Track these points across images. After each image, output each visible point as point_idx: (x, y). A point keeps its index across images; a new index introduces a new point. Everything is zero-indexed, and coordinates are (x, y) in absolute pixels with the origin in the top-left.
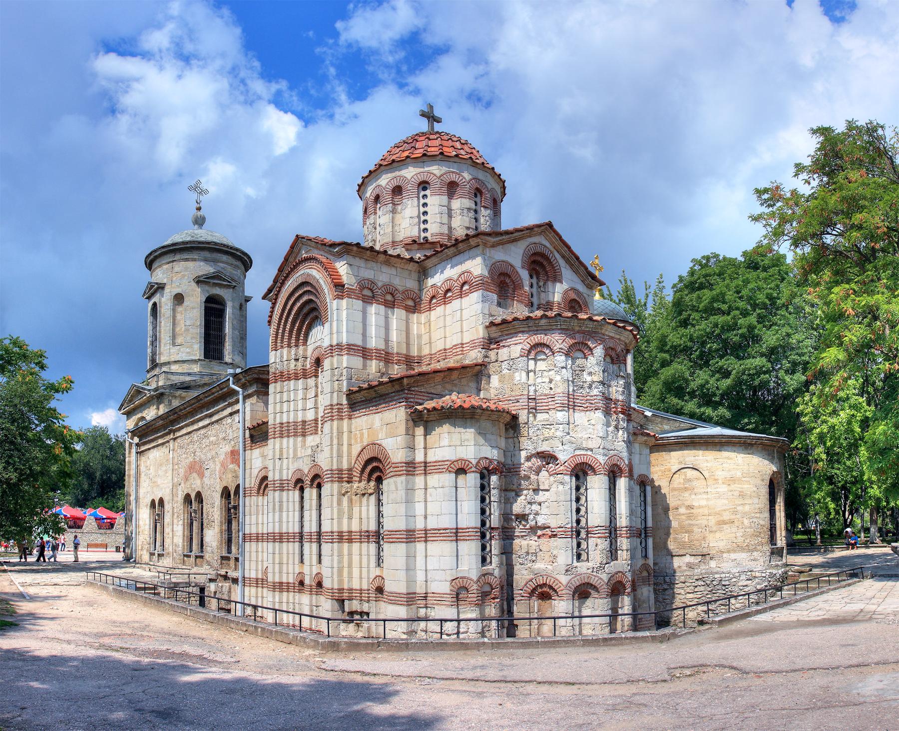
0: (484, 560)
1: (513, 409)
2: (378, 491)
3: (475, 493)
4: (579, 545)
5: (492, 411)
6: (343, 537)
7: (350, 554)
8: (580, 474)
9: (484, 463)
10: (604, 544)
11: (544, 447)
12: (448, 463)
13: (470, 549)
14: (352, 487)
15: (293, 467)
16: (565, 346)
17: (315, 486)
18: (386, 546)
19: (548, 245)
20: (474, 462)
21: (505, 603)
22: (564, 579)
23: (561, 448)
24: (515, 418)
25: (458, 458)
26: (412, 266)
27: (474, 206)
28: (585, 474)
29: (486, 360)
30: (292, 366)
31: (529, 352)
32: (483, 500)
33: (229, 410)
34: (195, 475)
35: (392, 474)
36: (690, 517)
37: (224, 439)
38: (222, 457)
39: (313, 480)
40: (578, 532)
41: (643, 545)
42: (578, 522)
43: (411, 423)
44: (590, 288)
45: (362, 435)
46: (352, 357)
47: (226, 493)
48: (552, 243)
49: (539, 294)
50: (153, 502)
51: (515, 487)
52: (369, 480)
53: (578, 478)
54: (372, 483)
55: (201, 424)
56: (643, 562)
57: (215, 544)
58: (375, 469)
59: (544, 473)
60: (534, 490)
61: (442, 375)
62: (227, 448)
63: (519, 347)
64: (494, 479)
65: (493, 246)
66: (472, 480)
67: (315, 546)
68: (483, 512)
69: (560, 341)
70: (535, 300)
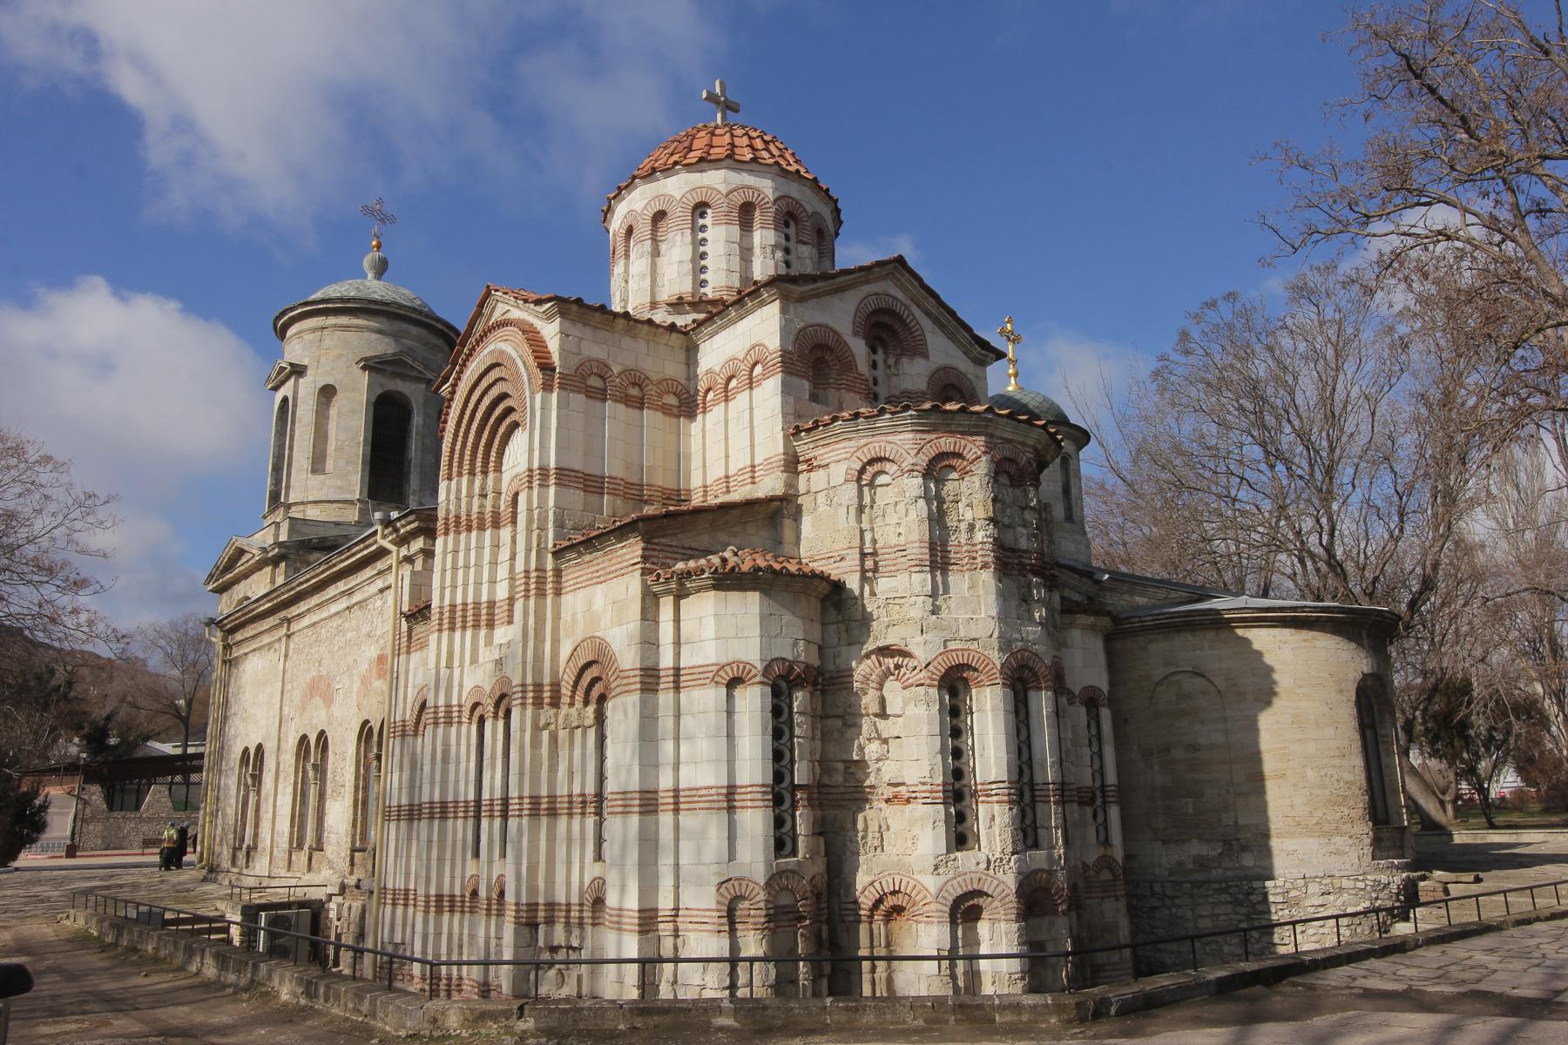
1: (834, 571)
2: (600, 719)
5: (792, 575)
9: (777, 669)
12: (715, 668)
13: (755, 822)
14: (556, 715)
16: (923, 461)
17: (501, 714)
20: (759, 666)
21: (825, 928)
23: (919, 639)
25: (730, 660)
30: (475, 508)
31: (862, 471)
32: (777, 734)
33: (380, 584)
34: (318, 700)
35: (618, 690)
37: (369, 635)
38: (364, 667)
39: (497, 705)
40: (957, 792)
44: (982, 363)
46: (564, 490)
47: (365, 732)
49: (888, 377)
51: (840, 712)
53: (954, 693)
54: (591, 709)
55: (334, 608)
59: (891, 686)
60: (876, 715)
61: (709, 516)
62: (371, 652)
63: (843, 467)
64: (799, 699)
68: (777, 756)
69: (913, 452)
70: (882, 391)
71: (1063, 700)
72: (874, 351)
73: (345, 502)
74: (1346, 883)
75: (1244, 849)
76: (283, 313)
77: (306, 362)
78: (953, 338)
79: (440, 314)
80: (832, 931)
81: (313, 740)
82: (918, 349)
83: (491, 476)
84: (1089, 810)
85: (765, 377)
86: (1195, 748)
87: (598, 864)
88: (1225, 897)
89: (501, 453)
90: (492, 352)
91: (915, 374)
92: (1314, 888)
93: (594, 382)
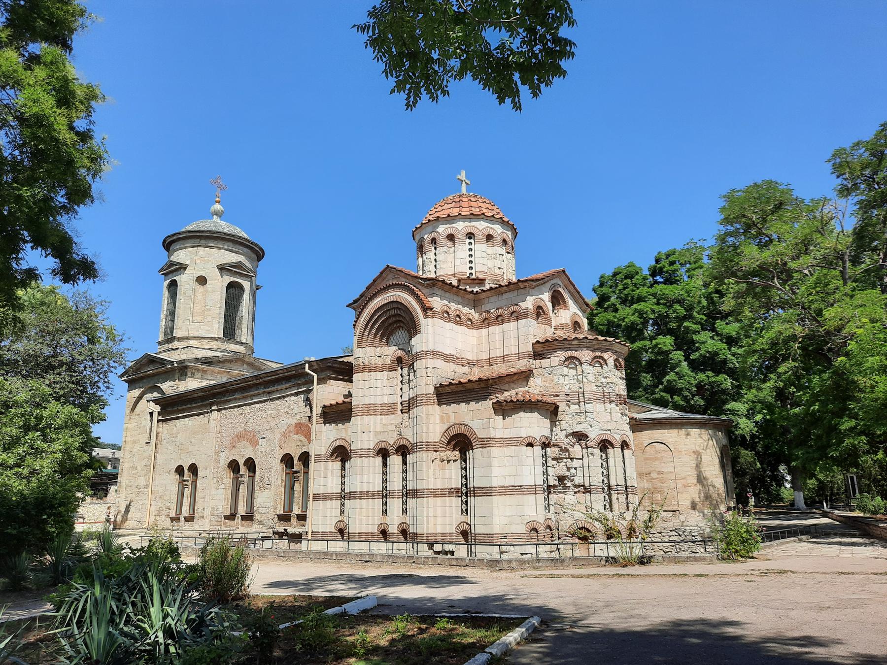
3: (540, 460)
6: (436, 493)
7: (435, 507)
11: (578, 428)
15: (380, 438)
18: (471, 500)
23: (590, 429)
24: (557, 407)
29: (533, 366)
36: (660, 480)
38: (284, 428)
45: (448, 417)
50: (180, 470)
57: (270, 505)
58: (461, 443)
66: (538, 449)
73: (211, 338)
76: (173, 235)
77: (188, 263)
78: (576, 302)
81: (241, 462)
82: (566, 307)
88: (674, 533)
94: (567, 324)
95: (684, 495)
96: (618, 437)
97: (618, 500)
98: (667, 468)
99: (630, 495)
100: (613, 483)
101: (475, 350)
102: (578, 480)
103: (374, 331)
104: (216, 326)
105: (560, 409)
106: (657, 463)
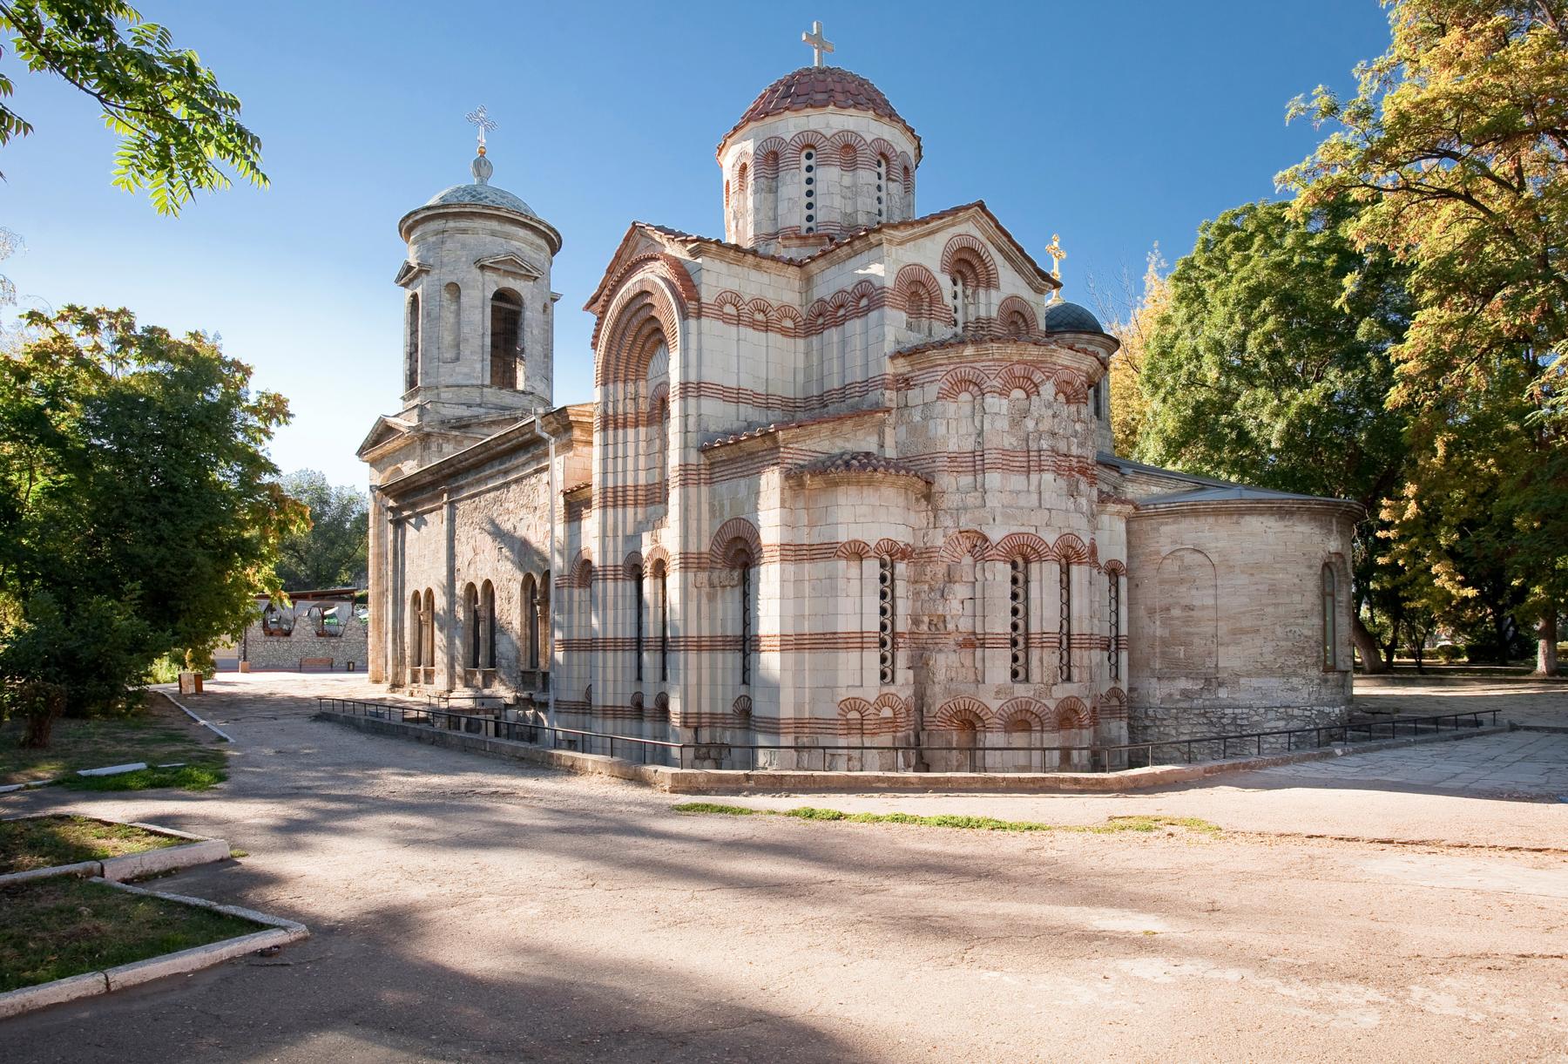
0: (883, 675)
4: (1015, 659)
8: (1020, 561)
10: (1052, 659)
11: (966, 522)
19: (978, 235)
22: (994, 705)
26: (792, 270)
27: (875, 181)
28: (1027, 561)
41: (1113, 660)
42: (1015, 627)
43: (787, 493)
45: (722, 506)
48: (984, 232)
52: (733, 568)
53: (1014, 566)
54: (736, 574)
56: (1112, 685)
64: (901, 568)
65: (901, 243)
66: (872, 568)
67: (659, 655)
70: (960, 317)
71: (1095, 571)
72: (955, 283)
74: (1296, 712)
75: (1220, 685)
77: (431, 261)
79: (540, 217)
80: (917, 736)
83: (642, 383)
84: (1106, 654)
85: (868, 309)
86: (1190, 608)
87: (743, 687)
89: (647, 365)
90: (641, 281)
91: (989, 304)
92: (1271, 715)
93: (729, 309)
94: (989, 319)
95: (1232, 649)
96: (1051, 538)
97: (1043, 662)
98: (1202, 598)
99: (1076, 653)
100: (1034, 628)
101: (801, 378)
102: (965, 625)
103: (624, 354)
104: (478, 366)
105: (935, 488)
106: (1183, 589)
